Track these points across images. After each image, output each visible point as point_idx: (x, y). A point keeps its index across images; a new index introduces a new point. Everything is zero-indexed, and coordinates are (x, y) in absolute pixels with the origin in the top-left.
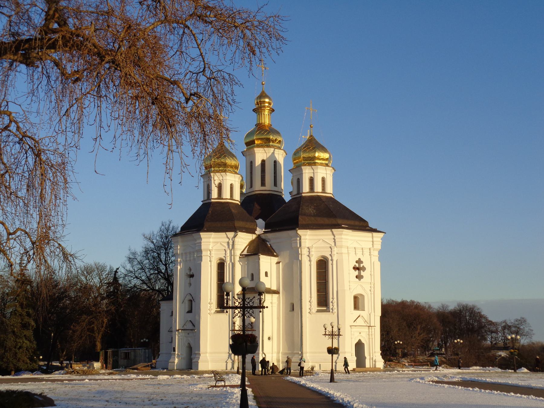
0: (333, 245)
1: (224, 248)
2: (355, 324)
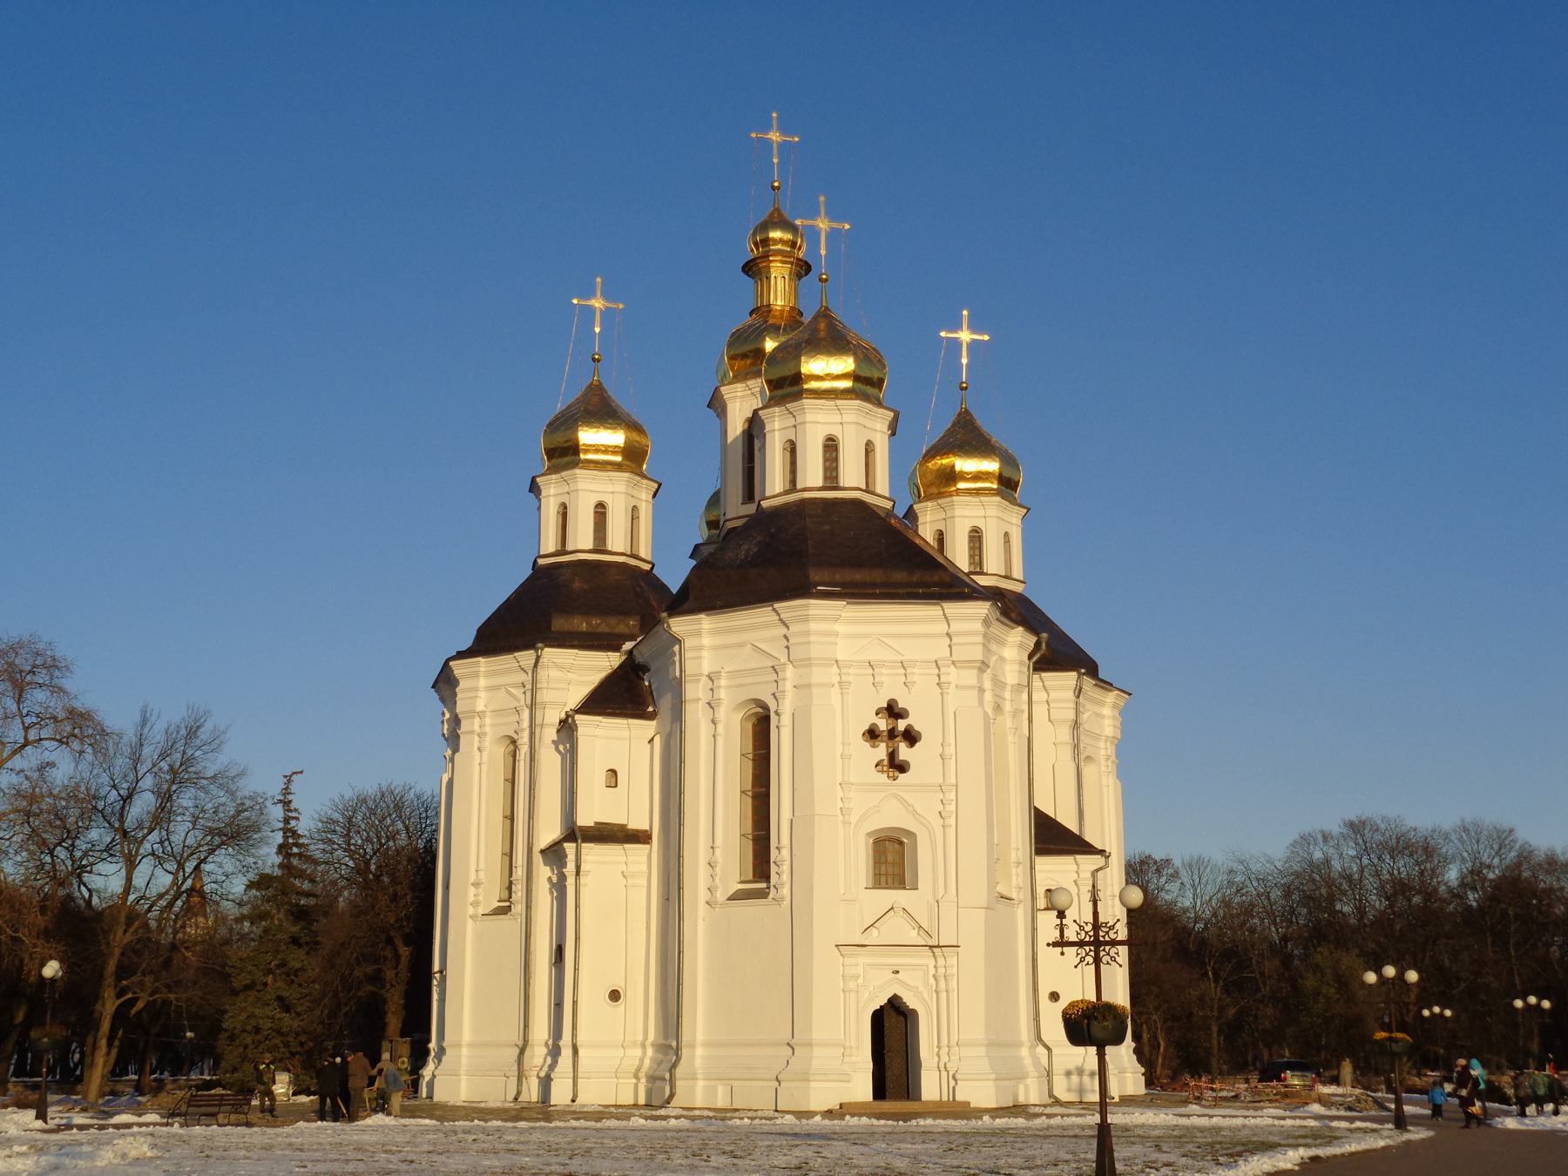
0: (783, 659)
1: (516, 704)
2: (874, 937)
